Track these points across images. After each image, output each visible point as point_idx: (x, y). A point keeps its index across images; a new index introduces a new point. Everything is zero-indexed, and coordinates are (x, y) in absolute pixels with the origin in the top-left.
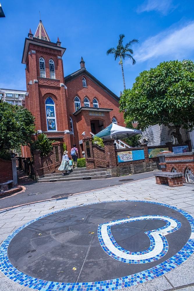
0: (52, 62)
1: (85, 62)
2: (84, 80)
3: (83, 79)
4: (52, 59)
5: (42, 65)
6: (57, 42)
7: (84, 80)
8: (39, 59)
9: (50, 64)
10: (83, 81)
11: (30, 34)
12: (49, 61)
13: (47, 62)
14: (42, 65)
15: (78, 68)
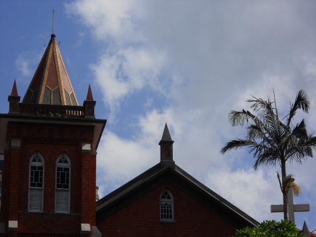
0: (66, 162)
1: (173, 142)
2: (169, 197)
3: (166, 193)
4: (65, 153)
5: (37, 173)
6: (85, 102)
7: (169, 197)
8: (29, 161)
9: (60, 169)
10: (165, 201)
11: (13, 98)
12: (58, 160)
13: (50, 164)
14: (37, 171)
15: (153, 158)
